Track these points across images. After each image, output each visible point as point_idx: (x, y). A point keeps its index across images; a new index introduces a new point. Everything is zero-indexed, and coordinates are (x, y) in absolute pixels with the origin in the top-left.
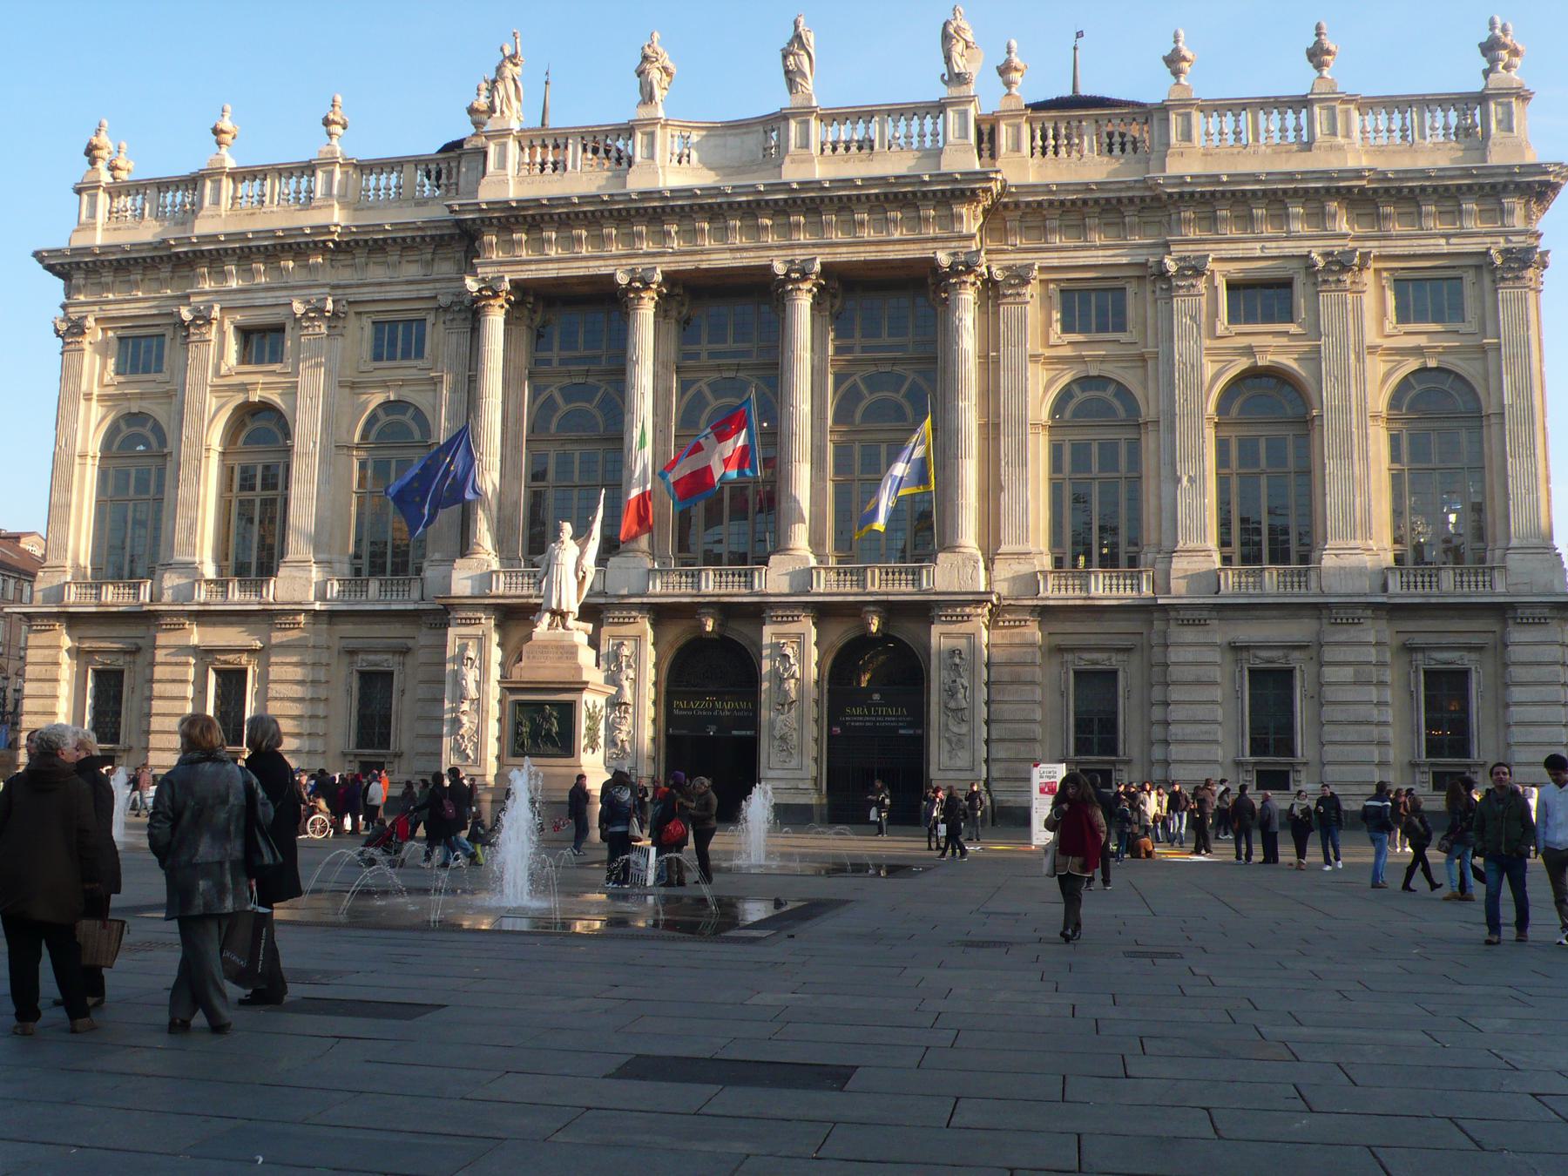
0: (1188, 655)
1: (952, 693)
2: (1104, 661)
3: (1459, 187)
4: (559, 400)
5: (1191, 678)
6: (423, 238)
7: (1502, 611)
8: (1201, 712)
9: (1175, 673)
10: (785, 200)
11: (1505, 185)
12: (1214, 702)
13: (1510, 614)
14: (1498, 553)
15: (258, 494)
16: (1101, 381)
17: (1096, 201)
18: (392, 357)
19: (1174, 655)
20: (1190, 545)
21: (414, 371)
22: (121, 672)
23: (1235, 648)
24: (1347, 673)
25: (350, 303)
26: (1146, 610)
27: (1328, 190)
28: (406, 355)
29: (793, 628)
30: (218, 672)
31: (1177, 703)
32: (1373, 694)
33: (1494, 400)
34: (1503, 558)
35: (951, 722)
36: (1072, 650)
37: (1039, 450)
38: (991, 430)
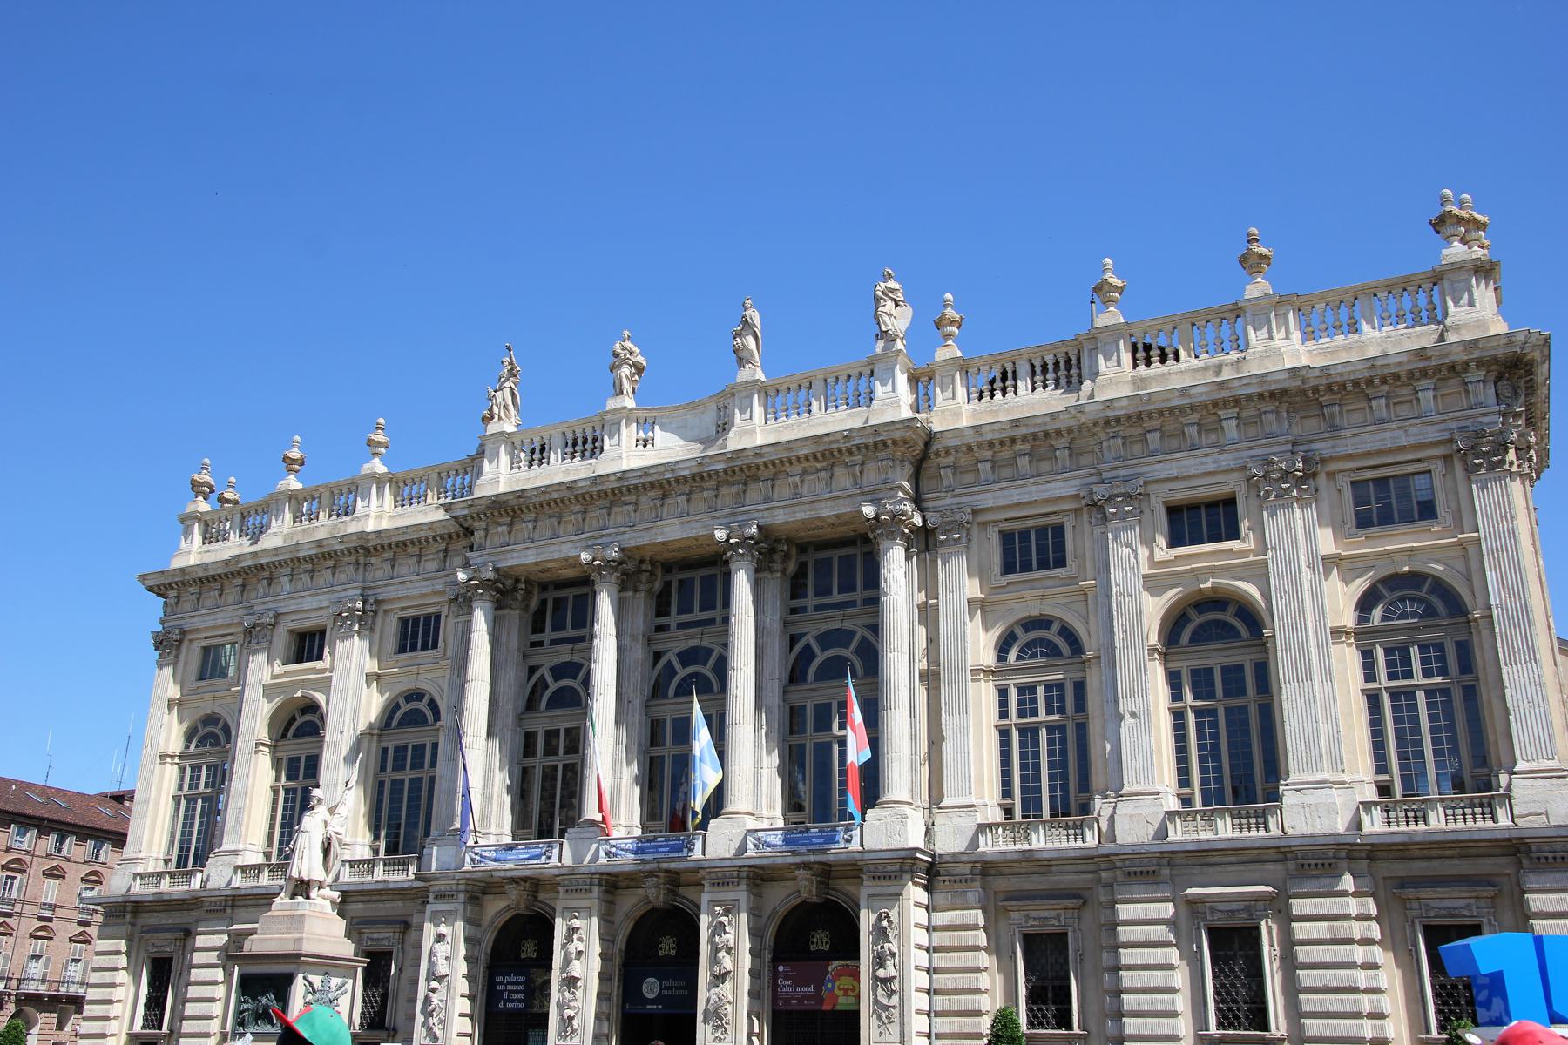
1: (880, 961)
3: (1411, 374)
4: (549, 678)
5: (1142, 938)
6: (434, 538)
8: (1156, 978)
10: (725, 471)
11: (1467, 363)
16: (1043, 622)
17: (1024, 439)
18: (413, 649)
20: (1137, 788)
22: (171, 959)
24: (1321, 929)
25: (377, 602)
27: (1261, 396)
28: (425, 647)
29: (731, 895)
33: (1480, 601)
35: (880, 991)
37: (984, 696)
38: (931, 678)
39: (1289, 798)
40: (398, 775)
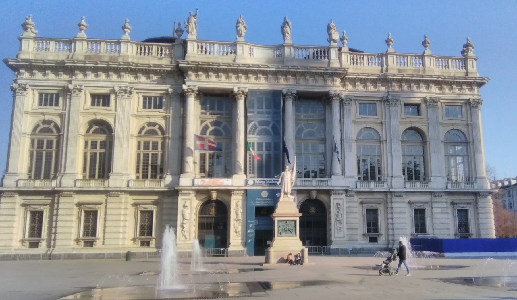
0: (398, 205)
2: (375, 206)
7: (476, 194)
9: (395, 210)
12: (405, 218)
13: (478, 194)
14: (474, 179)
15: (98, 151)
18: (150, 107)
19: (394, 205)
21: (158, 113)
23: (410, 203)
24: (439, 210)
26: (386, 193)
30: (85, 212)
31: (396, 218)
32: (445, 216)
34: (476, 179)
36: (366, 203)
39: (432, 180)
40: (146, 151)
